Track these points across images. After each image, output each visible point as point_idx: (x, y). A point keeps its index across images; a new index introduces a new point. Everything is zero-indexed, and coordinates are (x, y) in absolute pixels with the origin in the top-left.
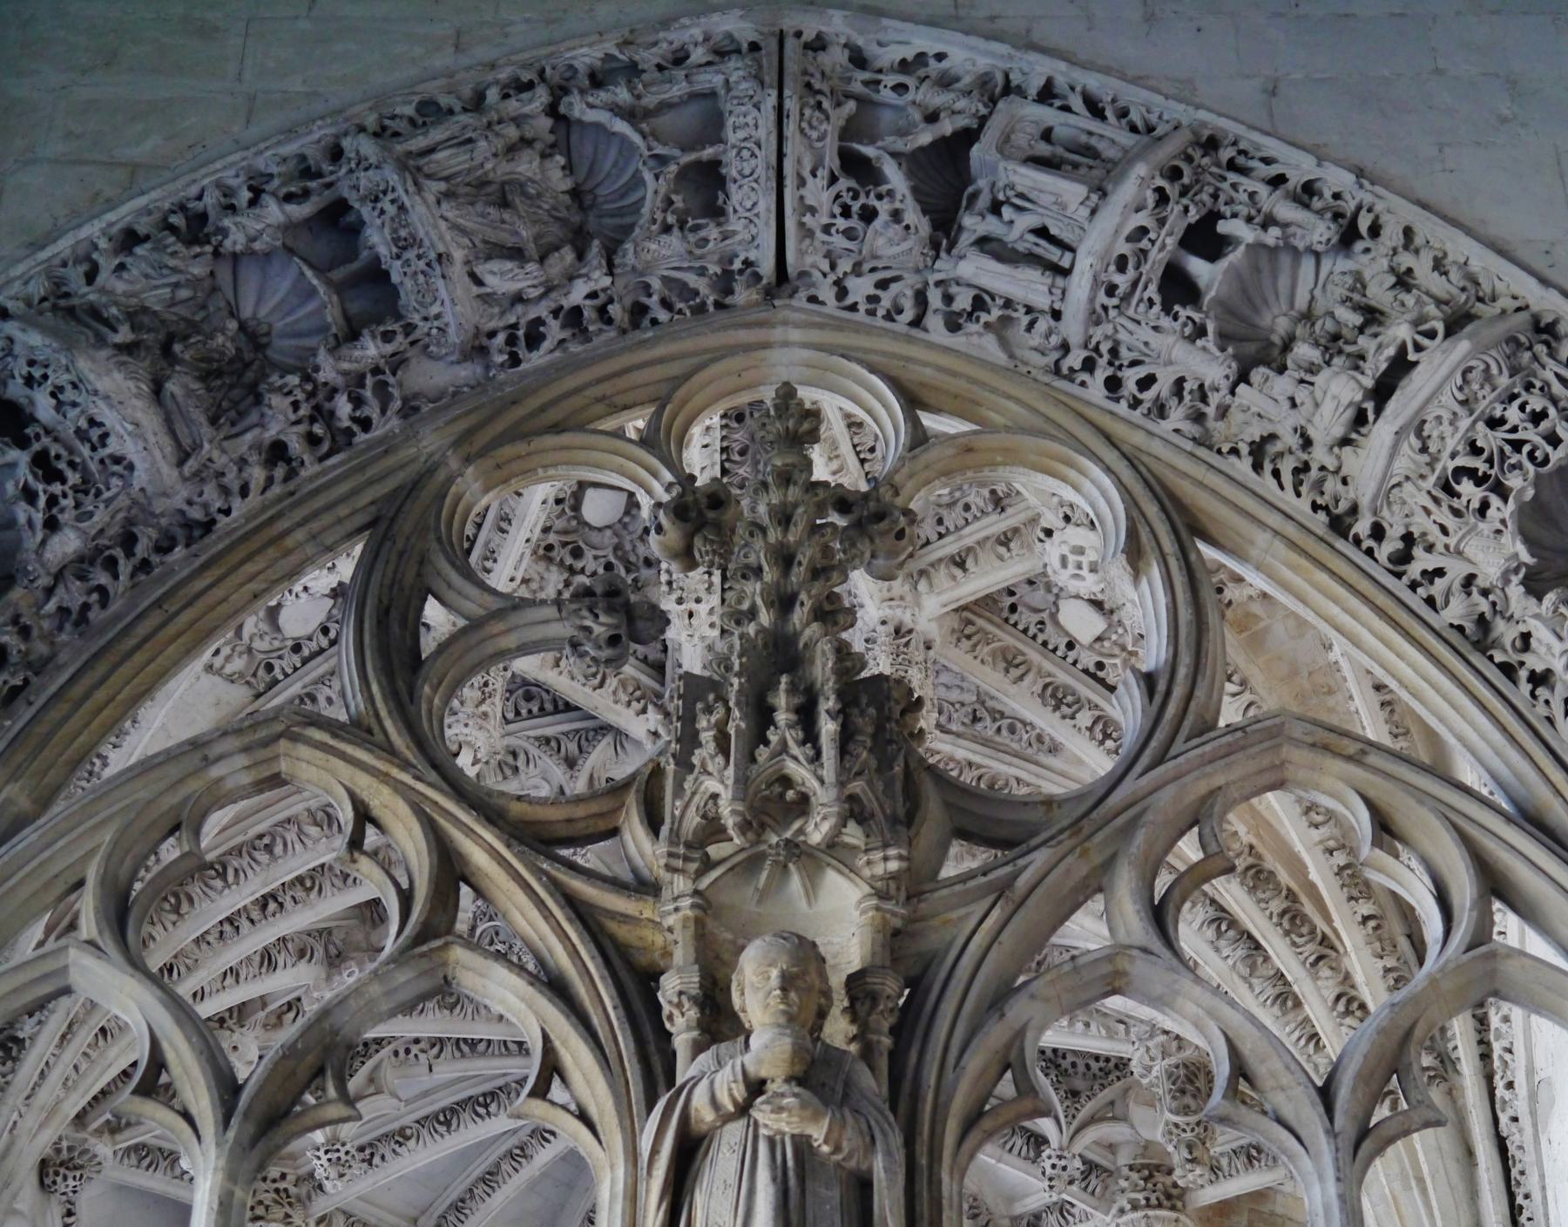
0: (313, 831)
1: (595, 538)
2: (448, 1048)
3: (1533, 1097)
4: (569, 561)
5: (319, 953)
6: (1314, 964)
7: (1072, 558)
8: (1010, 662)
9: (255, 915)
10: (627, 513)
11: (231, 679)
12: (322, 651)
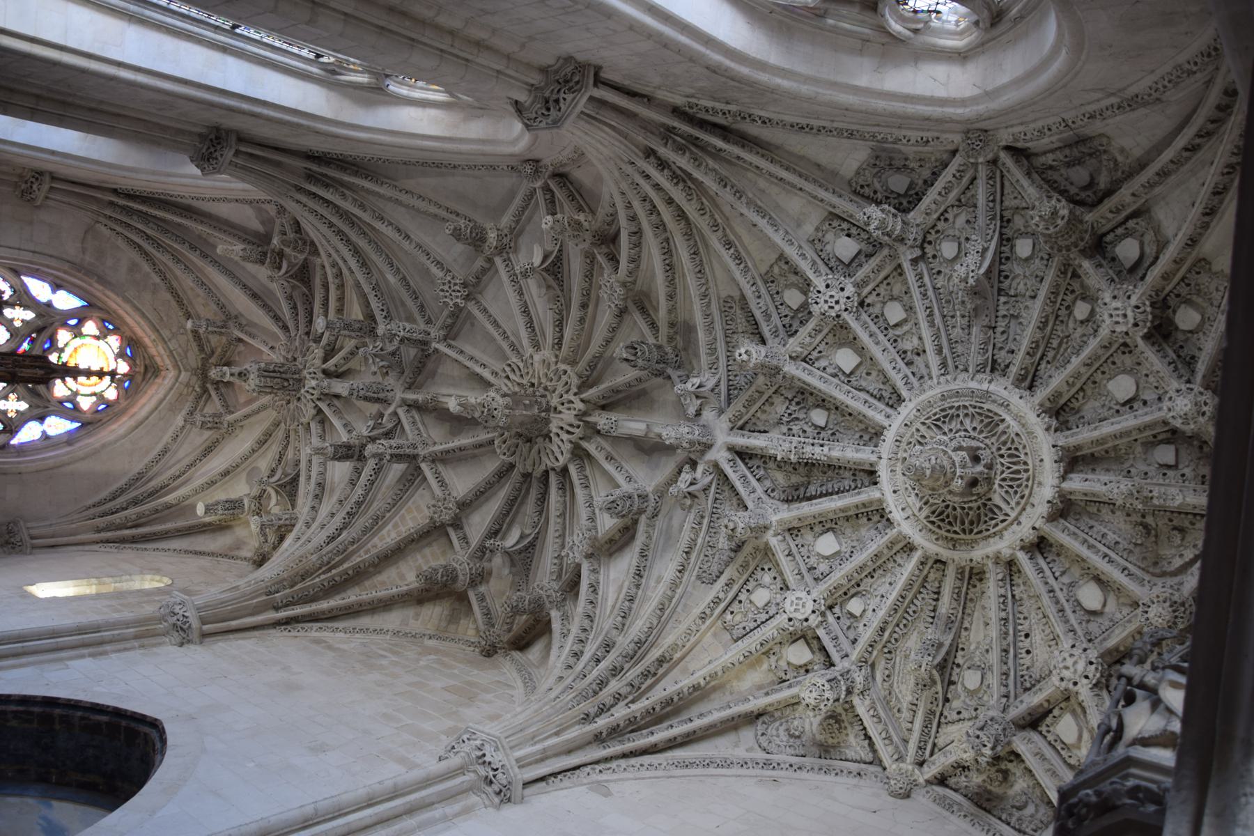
2: (558, 317)
3: (598, 782)
4: (796, 400)
6: (631, 685)
8: (745, 566)
9: (667, 262)
10: (813, 424)
11: (771, 266)
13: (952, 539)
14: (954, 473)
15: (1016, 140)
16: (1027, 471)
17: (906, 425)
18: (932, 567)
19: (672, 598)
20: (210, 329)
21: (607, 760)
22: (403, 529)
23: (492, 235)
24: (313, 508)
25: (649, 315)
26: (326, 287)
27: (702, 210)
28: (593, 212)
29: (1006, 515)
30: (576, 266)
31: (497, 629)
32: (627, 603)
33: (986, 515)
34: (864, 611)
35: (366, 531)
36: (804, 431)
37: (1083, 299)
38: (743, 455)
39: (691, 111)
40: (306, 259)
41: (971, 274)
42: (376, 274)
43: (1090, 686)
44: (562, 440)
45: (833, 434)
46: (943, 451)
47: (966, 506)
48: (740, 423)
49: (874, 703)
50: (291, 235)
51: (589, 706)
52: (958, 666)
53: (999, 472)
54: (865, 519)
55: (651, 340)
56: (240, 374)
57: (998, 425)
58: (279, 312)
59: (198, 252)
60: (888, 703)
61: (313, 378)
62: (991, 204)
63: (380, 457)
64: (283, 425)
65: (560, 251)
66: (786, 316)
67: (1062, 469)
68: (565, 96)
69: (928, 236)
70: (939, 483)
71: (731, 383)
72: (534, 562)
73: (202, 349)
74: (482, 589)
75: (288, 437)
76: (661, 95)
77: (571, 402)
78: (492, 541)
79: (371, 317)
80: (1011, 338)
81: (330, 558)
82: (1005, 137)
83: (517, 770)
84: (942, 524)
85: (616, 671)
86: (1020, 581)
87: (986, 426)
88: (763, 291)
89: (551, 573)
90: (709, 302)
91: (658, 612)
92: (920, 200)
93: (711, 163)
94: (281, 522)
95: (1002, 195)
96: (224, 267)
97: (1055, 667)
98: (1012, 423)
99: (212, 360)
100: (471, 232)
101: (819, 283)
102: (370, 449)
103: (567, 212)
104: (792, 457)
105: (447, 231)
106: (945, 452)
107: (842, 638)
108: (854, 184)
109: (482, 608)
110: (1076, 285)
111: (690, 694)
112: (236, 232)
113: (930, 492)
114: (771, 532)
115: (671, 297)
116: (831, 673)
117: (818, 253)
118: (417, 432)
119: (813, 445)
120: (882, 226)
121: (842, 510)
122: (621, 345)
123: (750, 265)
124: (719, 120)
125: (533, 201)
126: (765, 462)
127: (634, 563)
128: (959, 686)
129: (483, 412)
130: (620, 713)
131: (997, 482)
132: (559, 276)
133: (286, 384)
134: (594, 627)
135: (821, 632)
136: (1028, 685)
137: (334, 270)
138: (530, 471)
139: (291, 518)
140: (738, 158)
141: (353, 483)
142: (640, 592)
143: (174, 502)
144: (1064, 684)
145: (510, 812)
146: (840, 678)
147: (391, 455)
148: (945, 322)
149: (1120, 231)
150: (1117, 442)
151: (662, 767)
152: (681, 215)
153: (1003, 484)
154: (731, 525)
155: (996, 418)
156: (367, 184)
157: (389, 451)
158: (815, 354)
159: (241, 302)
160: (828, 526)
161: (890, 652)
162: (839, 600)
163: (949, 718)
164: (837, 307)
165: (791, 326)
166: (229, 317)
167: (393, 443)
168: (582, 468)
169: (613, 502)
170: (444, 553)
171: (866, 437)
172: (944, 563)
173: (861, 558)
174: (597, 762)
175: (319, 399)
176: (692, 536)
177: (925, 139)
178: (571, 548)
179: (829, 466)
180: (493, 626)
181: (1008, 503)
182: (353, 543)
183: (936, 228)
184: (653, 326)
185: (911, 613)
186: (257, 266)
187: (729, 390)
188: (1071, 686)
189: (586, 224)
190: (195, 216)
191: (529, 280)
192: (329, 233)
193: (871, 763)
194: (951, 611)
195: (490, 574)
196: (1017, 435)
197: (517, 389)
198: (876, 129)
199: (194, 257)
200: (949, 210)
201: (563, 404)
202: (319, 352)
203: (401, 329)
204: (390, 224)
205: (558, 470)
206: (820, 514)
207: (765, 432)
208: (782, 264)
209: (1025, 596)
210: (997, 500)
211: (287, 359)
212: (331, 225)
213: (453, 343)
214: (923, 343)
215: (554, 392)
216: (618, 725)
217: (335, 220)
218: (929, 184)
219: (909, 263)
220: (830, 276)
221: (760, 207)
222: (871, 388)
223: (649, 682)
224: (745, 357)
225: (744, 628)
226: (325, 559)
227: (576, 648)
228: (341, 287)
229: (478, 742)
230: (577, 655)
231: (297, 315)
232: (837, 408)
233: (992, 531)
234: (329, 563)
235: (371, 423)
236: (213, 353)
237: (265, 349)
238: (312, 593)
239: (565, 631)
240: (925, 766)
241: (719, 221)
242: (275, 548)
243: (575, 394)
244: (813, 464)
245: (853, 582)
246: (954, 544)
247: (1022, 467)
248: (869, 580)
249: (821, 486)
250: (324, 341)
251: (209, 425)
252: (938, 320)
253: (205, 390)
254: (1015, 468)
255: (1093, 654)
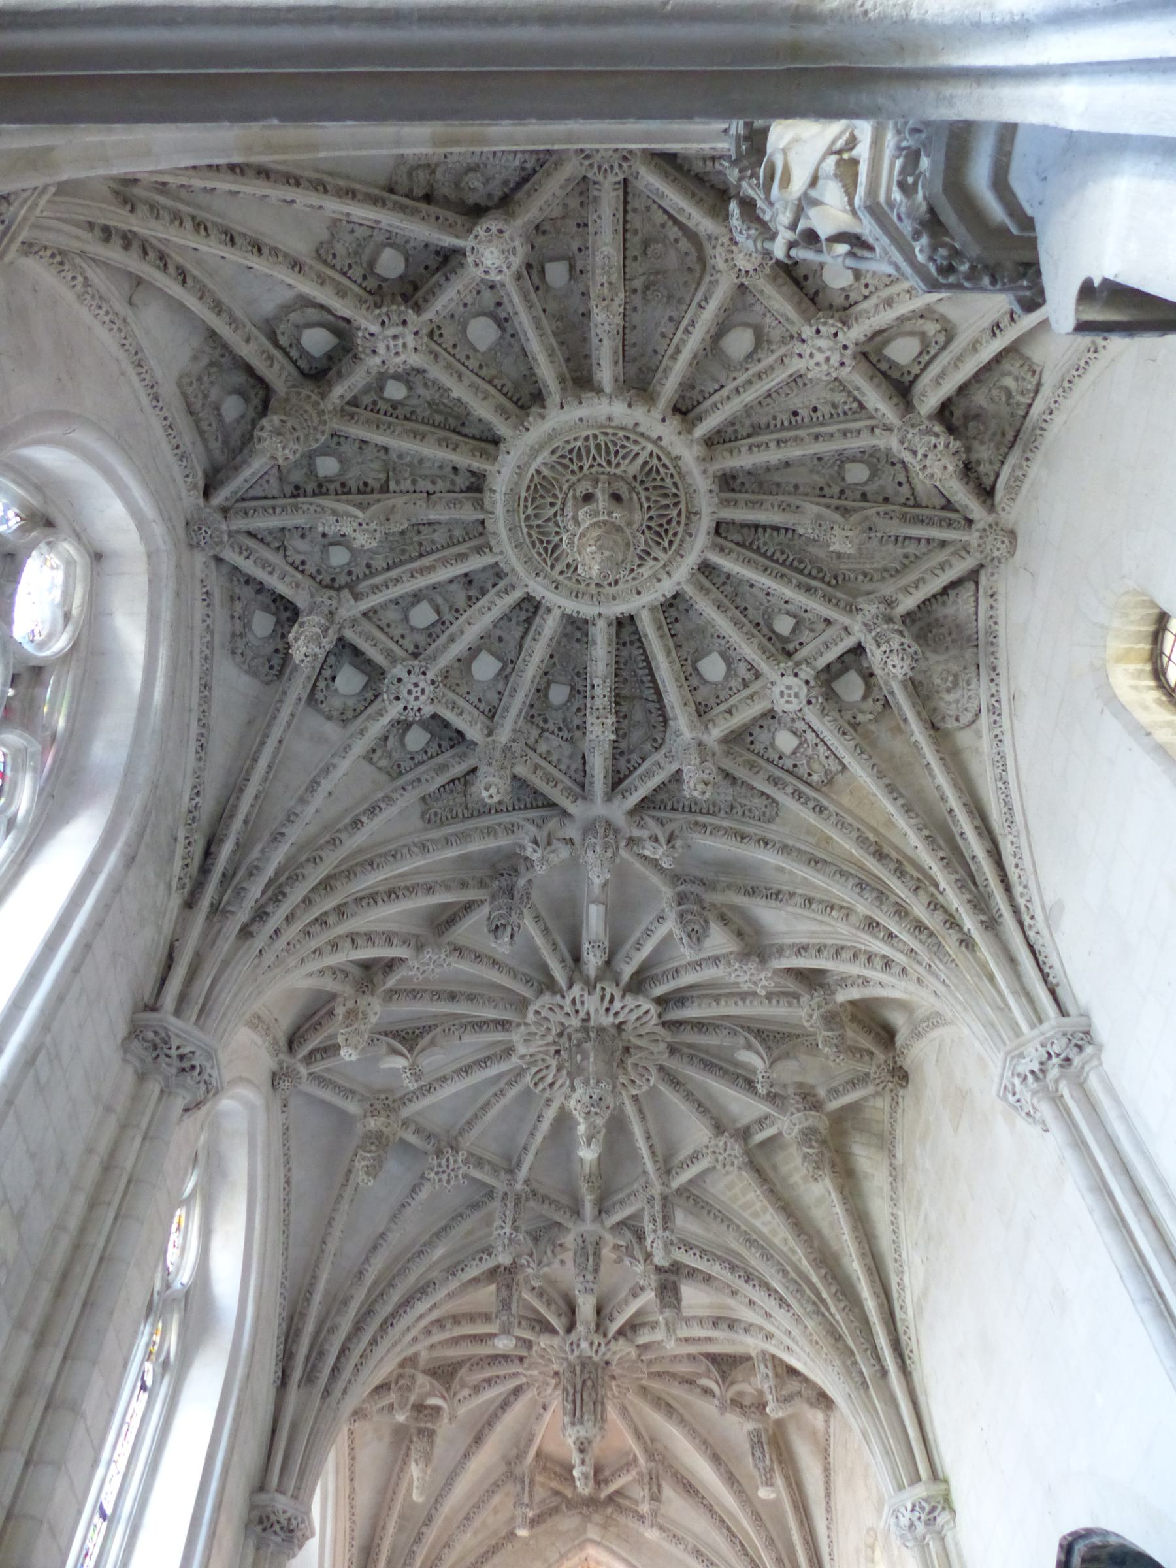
0: (416, 850)
1: (554, 713)
2: (469, 1028)
3: (1047, 919)
4: (541, 724)
5: (413, 943)
7: (786, 692)
8: (752, 766)
9: (386, 899)
10: (569, 700)
11: (380, 769)
12: (424, 762)
13: (688, 518)
14: (605, 523)
15: (195, 487)
16: (595, 437)
17: (556, 588)
18: (725, 538)
19: (799, 850)
20: (526, 1500)
21: (1016, 911)
22: (758, 1205)
23: (373, 1123)
24: (746, 1330)
25: (455, 914)
26: (456, 1341)
27: (314, 860)
28: (333, 997)
29: (651, 454)
30: (406, 1010)
31: (871, 1069)
32: (814, 906)
33: (655, 479)
34: (788, 613)
35: (767, 1256)
36: (579, 710)
37: (381, 389)
38: (617, 782)
39: (188, 887)
40: (424, 1372)
41: (364, 526)
42: (434, 1274)
43: (845, 329)
44: (622, 1008)
45: (578, 674)
46: (580, 538)
47: (646, 505)
48: (578, 790)
49: (900, 589)
50: (393, 1397)
51: (950, 941)
52: (842, 492)
53: (601, 470)
54: (677, 625)
55: (485, 910)
56: (581, 1451)
57: (544, 477)
58: (498, 1403)
59: (424, 1530)
60: (897, 571)
61: (578, 1345)
62: (278, 510)
63: (668, 1244)
64: (644, 1382)
65: (386, 1034)
66: (440, 746)
67: (590, 395)
68: (174, 1047)
69: (324, 583)
70: (619, 540)
71: (529, 805)
72: (781, 1030)
73: (554, 1511)
74: (822, 1092)
75: (659, 1375)
76: (168, 926)
77: (574, 1002)
78: (759, 1086)
79: (493, 1273)
80: (438, 472)
81: (808, 1301)
82: (192, 499)
83: (1045, 1026)
84: (671, 533)
85: (901, 912)
86: (730, 430)
87: (547, 490)
88: (410, 776)
89: (790, 1005)
90: (431, 841)
91: (819, 865)
92: (281, 597)
93: (255, 853)
94: (770, 1374)
95: (266, 498)
96: (443, 1489)
97: (828, 374)
98: (540, 460)
99: (569, 1493)
100: (370, 1152)
101: (394, 711)
102: (659, 1259)
103: (336, 1029)
104: (609, 721)
105: (370, 1184)
106: (582, 535)
107: (825, 637)
108: (269, 678)
109: (846, 1091)
110: (367, 400)
111: (917, 816)
112: (394, 1477)
113: (632, 549)
114: (705, 738)
115: (429, 889)
116: (870, 646)
117: (357, 714)
118: (632, 1198)
119: (593, 698)
120: (316, 639)
121: (669, 654)
122: (493, 945)
123: (380, 795)
124: (198, 850)
125: (326, 1075)
126: (622, 753)
127: (763, 902)
128: (866, 489)
129: (596, 1113)
130: (955, 901)
131: (612, 470)
132: (417, 1032)
133: (589, 1383)
134: (849, 944)
135: (821, 663)
136: (855, 405)
137: (435, 1330)
138: (665, 1045)
139: (764, 1359)
140: (246, 822)
141: (708, 1279)
142: (799, 891)
143: (764, 1534)
144: (847, 361)
145: (1102, 1028)
146: (874, 634)
147: (665, 1229)
148: (428, 554)
149: (294, 354)
150: (550, 333)
151: (1014, 840)
152: (326, 885)
153: (614, 463)
154: (701, 786)
155: (536, 480)
156: (318, 1297)
157: (660, 1232)
158: (482, 706)
159: (486, 1458)
160: (689, 669)
161: (836, 577)
162: (779, 645)
163: (909, 495)
164: (422, 685)
165: (451, 739)
166: (509, 1475)
167: (648, 1227)
168: (654, 980)
169: (689, 936)
170: (783, 1147)
171: (578, 635)
172: (718, 524)
173: (723, 624)
174: (1021, 923)
175: (605, 1335)
176: (721, 833)
177: (204, 597)
178: (755, 984)
179: (616, 675)
180: (867, 1075)
181: (637, 454)
182: (785, 1272)
183: (314, 574)
184: (468, 907)
185: (785, 556)
186: (439, 1441)
187: (538, 807)
188: (848, 352)
189: (350, 1004)
190: (377, 1540)
191: (424, 1071)
192: (385, 1344)
193: (977, 583)
194: (776, 508)
195: (801, 1085)
196: (553, 452)
197: (564, 1072)
198: (197, 657)
199: (431, 1535)
200: (290, 560)
201: (577, 1012)
202: (544, 1341)
203: (501, 1232)
204: (367, 1259)
205: (660, 1009)
206: (677, 680)
207: (584, 757)
208: (375, 757)
209: (747, 423)
210: (634, 468)
211: (557, 1385)
212: (374, 1342)
213: (514, 1161)
214: (456, 577)
215: (562, 1024)
216: (969, 901)
217: (366, 1338)
218: (260, 588)
219: (359, 603)
220: (385, 696)
221: (307, 790)
222: (518, 635)
223: (909, 868)
224: (493, 791)
225: (827, 757)
226: (810, 1308)
227: (878, 962)
228: (456, 1319)
229: (1017, 1081)
230: (888, 963)
231: (498, 1377)
232: (546, 673)
233: (672, 470)
234: (814, 1303)
235: (627, 1261)
236: (557, 1493)
237: (548, 1416)
238: (856, 1324)
239: (860, 981)
240: (971, 517)
241: (327, 838)
242: (806, 1380)
243: (563, 997)
244: (617, 695)
245: (755, 632)
246: (693, 514)
247: (592, 443)
248: (750, 612)
249: (642, 682)
250: (527, 1335)
251: (655, 1489)
252: (426, 561)
253: (610, 1499)
254: (593, 451)
255: (807, 332)
